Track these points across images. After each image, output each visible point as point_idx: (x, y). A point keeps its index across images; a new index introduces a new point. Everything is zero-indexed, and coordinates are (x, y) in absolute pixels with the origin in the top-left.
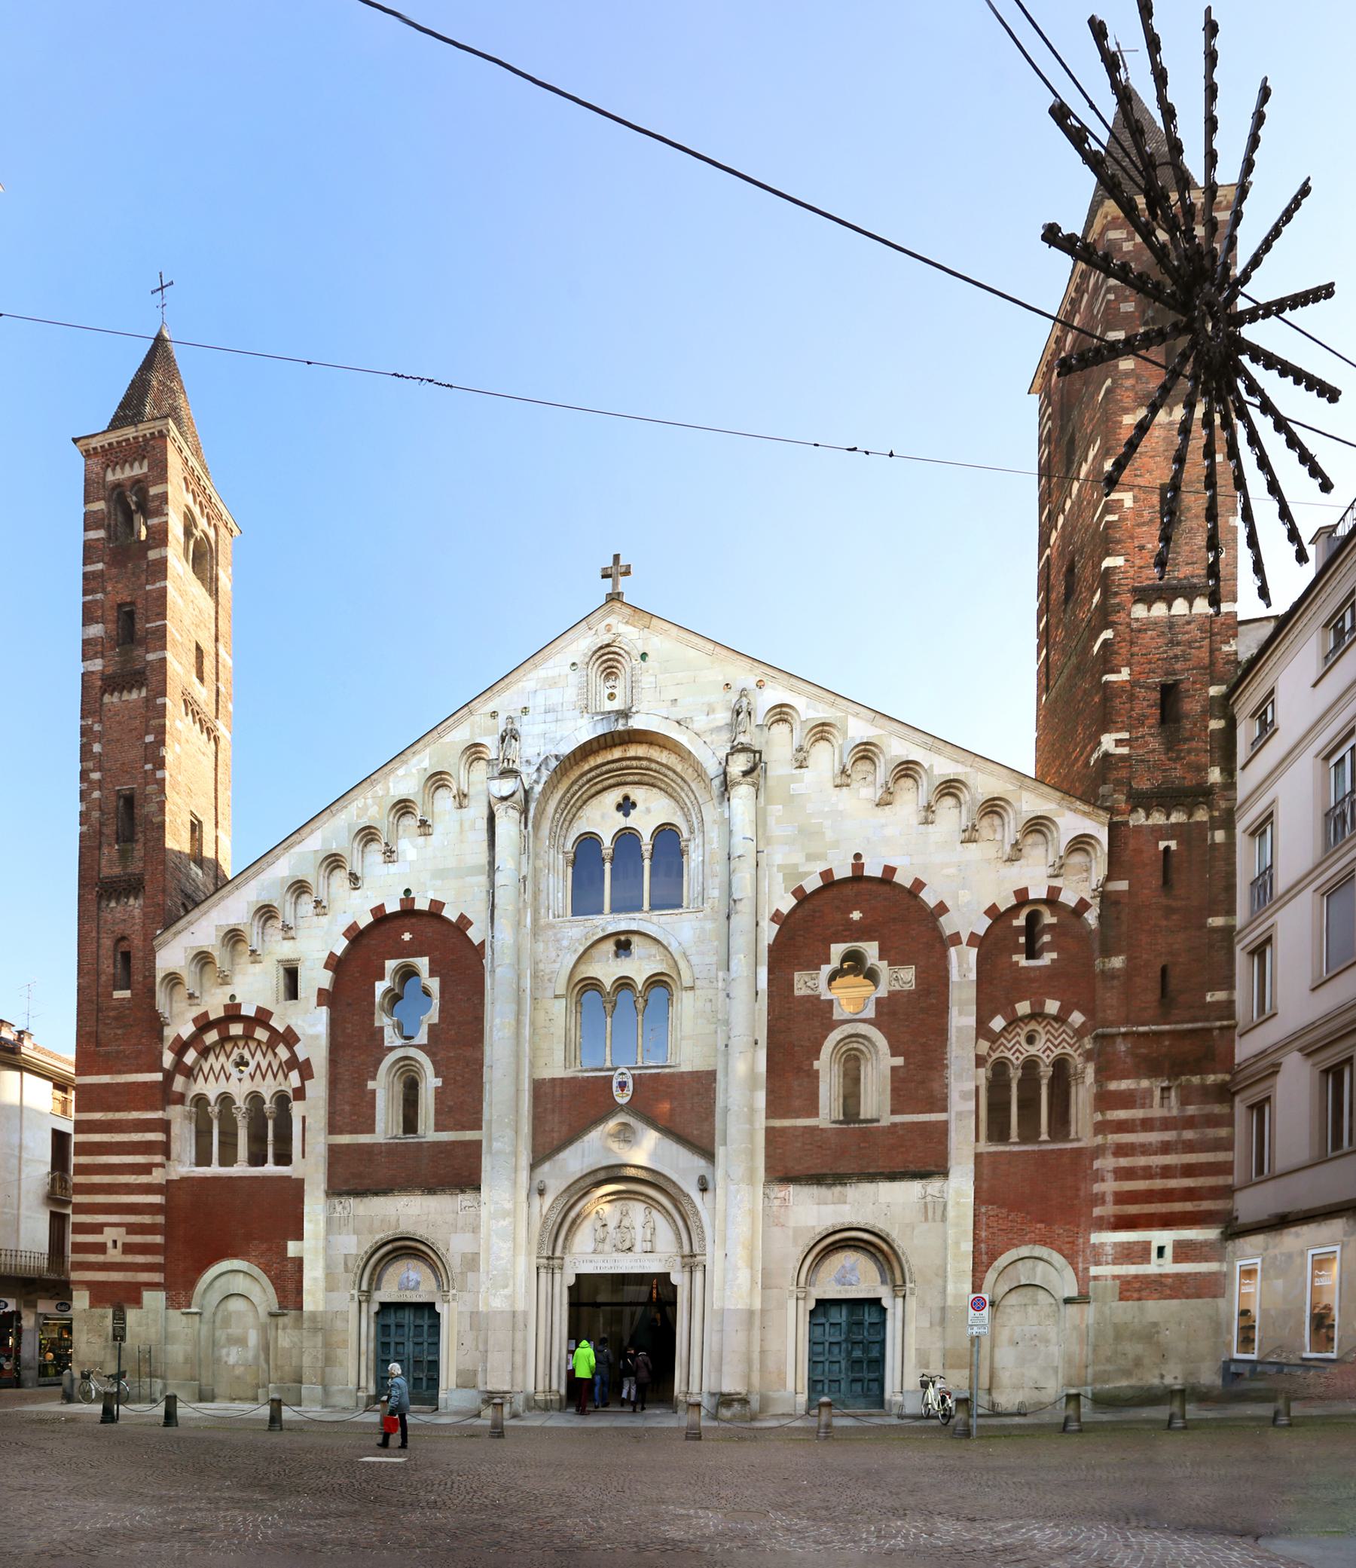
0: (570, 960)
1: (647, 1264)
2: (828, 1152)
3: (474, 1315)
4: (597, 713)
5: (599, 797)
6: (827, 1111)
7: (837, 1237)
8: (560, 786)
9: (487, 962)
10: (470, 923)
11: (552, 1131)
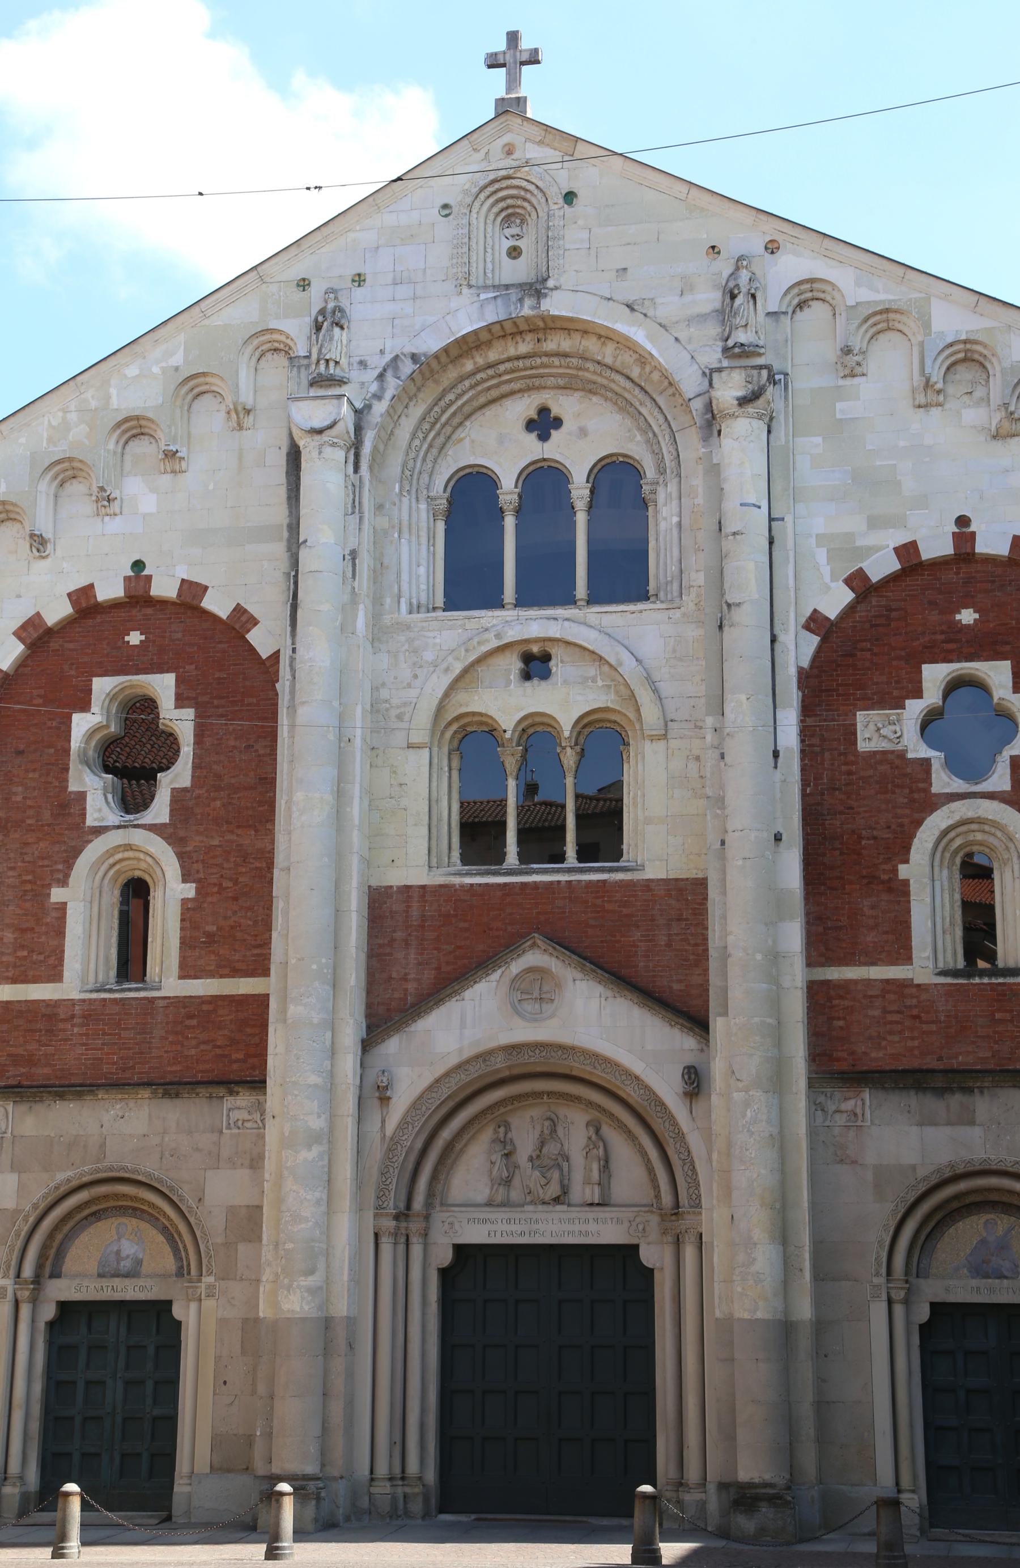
0: (439, 684)
1: (592, 1227)
2: (934, 1027)
3: (251, 1325)
4: (486, 287)
5: (494, 409)
6: (928, 952)
7: (963, 1186)
8: (421, 395)
9: (283, 687)
10: (255, 622)
11: (405, 979)
